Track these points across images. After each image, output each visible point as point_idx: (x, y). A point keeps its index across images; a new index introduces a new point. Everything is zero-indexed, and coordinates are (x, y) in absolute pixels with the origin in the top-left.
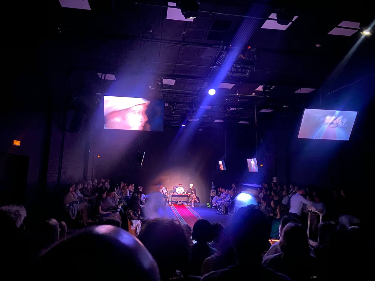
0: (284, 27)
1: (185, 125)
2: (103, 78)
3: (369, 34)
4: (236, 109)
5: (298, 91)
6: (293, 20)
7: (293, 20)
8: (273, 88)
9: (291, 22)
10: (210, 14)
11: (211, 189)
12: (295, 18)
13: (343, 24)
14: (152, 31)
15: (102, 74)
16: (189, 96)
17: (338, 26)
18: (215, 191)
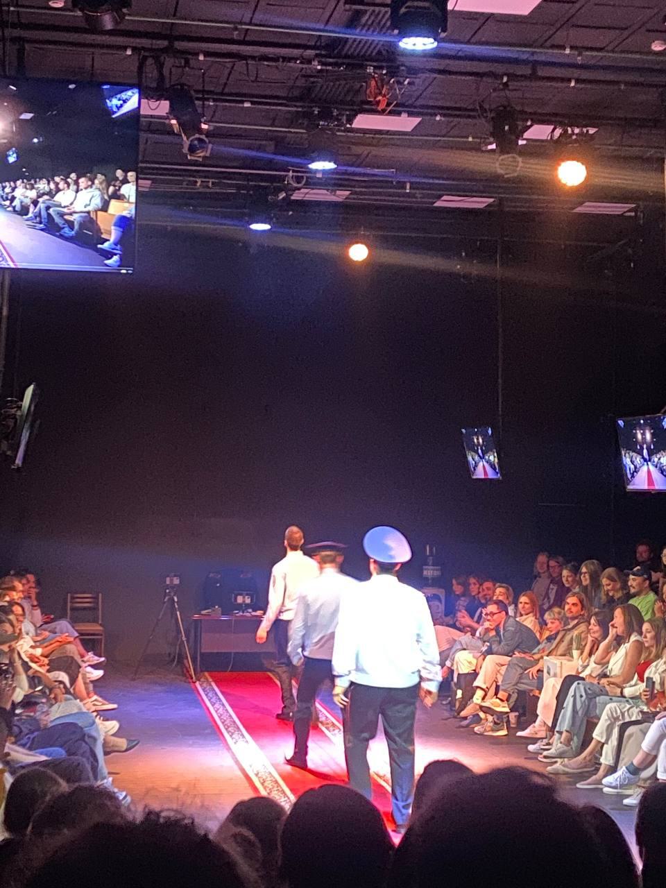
1: (266, 227)
4: (558, 132)
16: (290, 59)
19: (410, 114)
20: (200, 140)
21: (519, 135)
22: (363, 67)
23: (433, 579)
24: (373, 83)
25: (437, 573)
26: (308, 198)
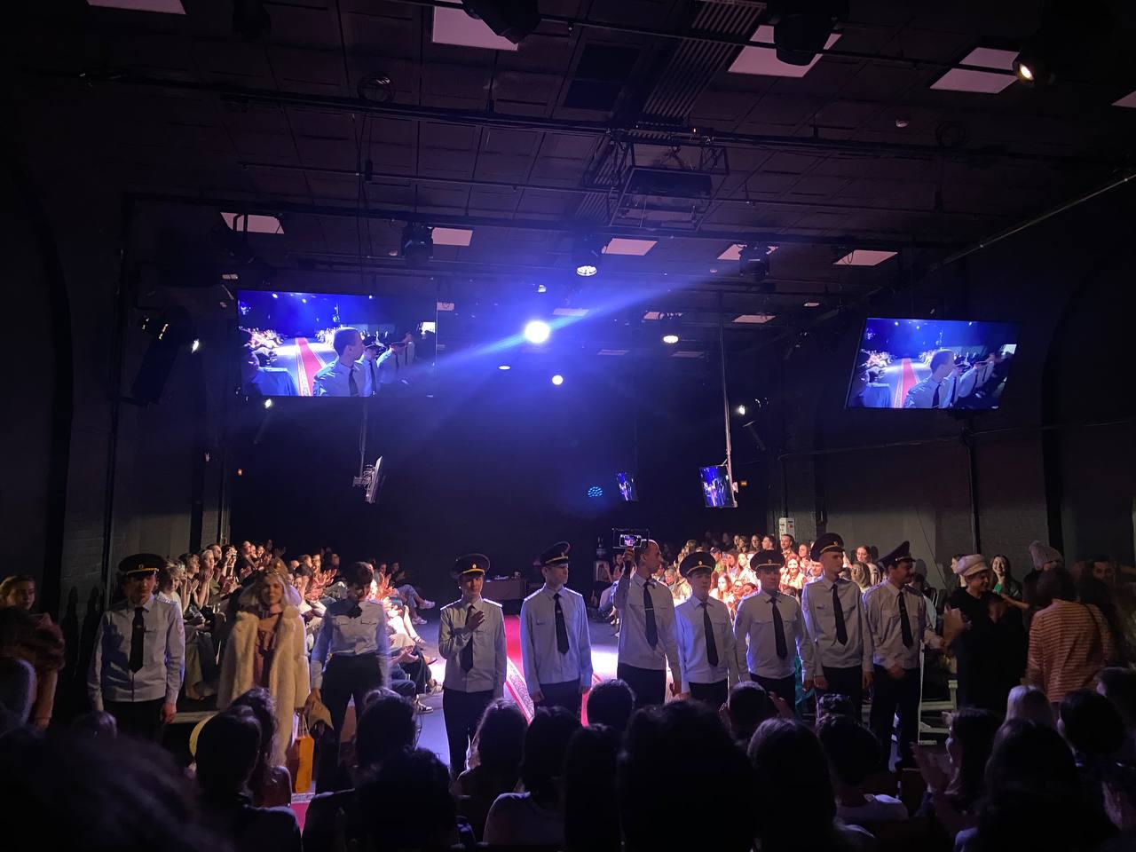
0: (799, 71)
2: (240, 228)
4: (662, 316)
5: (845, 258)
6: (827, 47)
7: (827, 47)
9: (820, 53)
10: (570, 29)
12: (833, 39)
13: (978, 56)
14: (388, 81)
15: (236, 215)
23: (603, 556)
25: (604, 553)
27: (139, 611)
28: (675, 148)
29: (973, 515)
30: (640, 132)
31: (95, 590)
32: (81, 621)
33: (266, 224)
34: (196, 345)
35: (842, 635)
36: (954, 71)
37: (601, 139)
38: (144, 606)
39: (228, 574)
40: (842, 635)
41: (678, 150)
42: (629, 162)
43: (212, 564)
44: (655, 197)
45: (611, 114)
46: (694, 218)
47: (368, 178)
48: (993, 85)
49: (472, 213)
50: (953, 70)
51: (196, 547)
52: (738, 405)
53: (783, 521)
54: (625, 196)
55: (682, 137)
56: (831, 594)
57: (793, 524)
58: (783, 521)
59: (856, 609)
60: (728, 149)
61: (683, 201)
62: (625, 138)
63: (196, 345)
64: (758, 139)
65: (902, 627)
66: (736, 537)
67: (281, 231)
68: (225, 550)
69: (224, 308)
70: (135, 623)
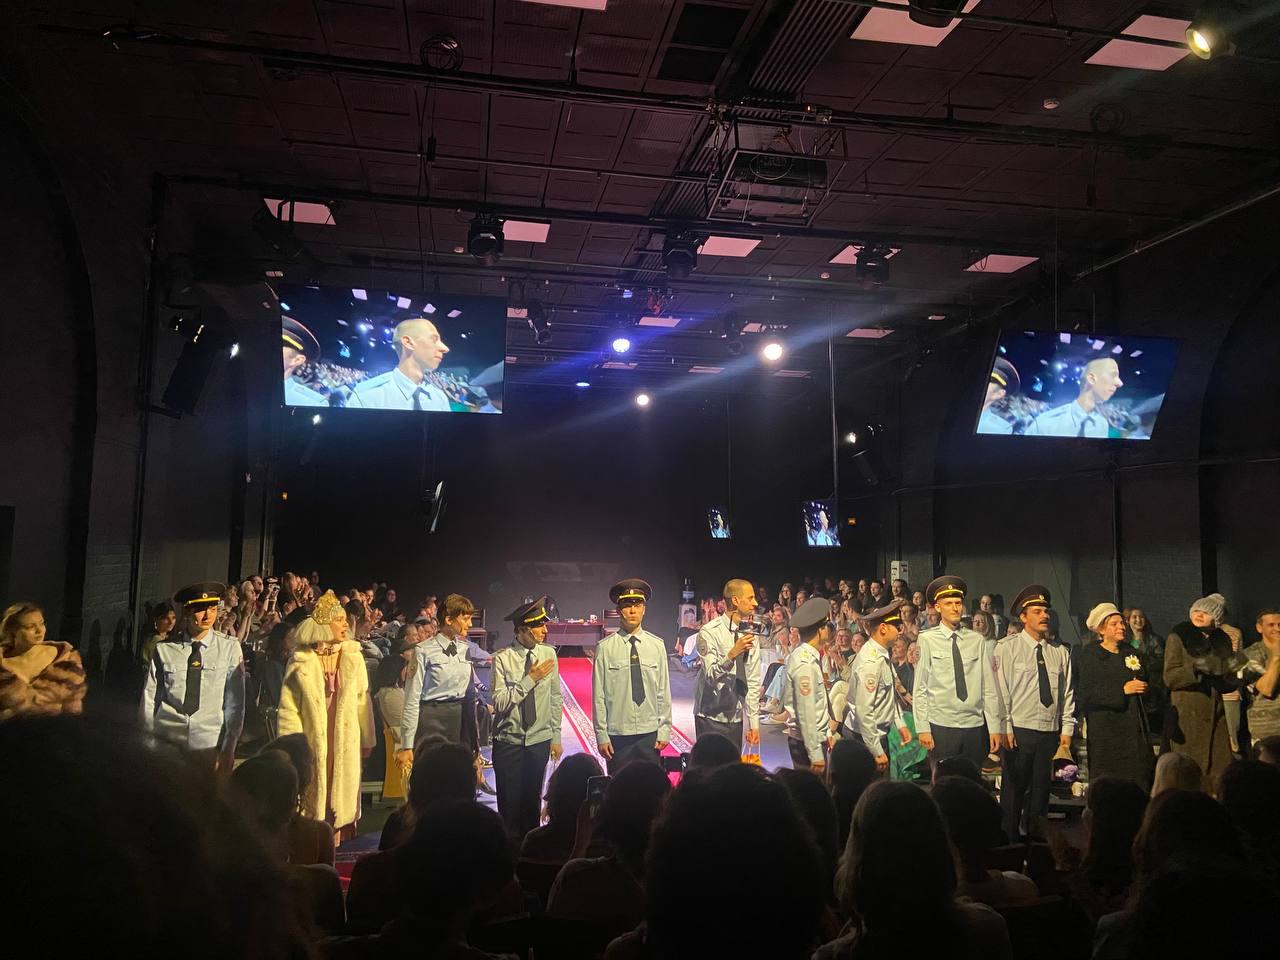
0: (931, 36)
1: (587, 385)
2: (285, 217)
3: (1204, 52)
4: (764, 328)
5: (978, 264)
6: (966, 10)
8: (891, 255)
11: (683, 603)
13: (1143, 25)
14: (455, 46)
17: (1124, 32)
18: (695, 608)
19: (675, 317)
20: (547, 333)
21: (741, 330)
22: (646, 289)
24: (651, 298)
25: (692, 596)
26: (612, 367)
27: (196, 647)
28: (786, 129)
29: (1115, 561)
30: (746, 109)
31: (122, 621)
32: (105, 656)
33: (315, 213)
34: (235, 350)
35: (962, 693)
36: (1115, 42)
37: (698, 119)
38: (202, 641)
39: (270, 609)
40: (962, 693)
41: (789, 131)
42: (731, 145)
43: (253, 597)
44: (761, 186)
45: (713, 88)
46: (805, 212)
47: (431, 156)
48: (1159, 60)
49: (549, 204)
50: (1114, 41)
51: (235, 578)
52: (848, 433)
53: (895, 564)
54: (726, 184)
55: (794, 117)
56: (951, 644)
57: (907, 568)
58: (895, 564)
59: (979, 661)
60: (847, 132)
61: (789, 192)
62: (727, 116)
63: (235, 350)
64: (882, 122)
65: (1040, 680)
66: (842, 582)
67: (332, 222)
68: (266, 584)
69: (266, 301)
70: (190, 661)
